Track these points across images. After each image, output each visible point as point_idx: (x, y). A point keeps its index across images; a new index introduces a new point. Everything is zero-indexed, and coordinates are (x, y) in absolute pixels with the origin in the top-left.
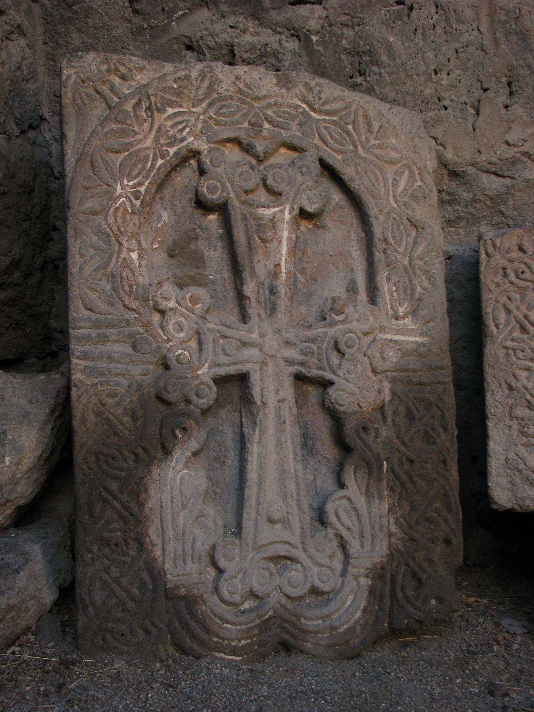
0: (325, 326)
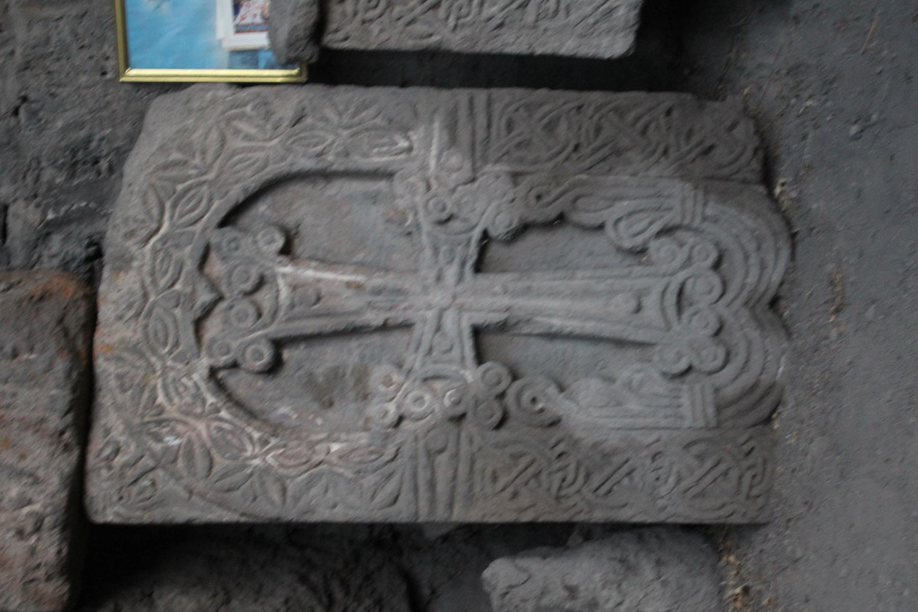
0: (420, 234)
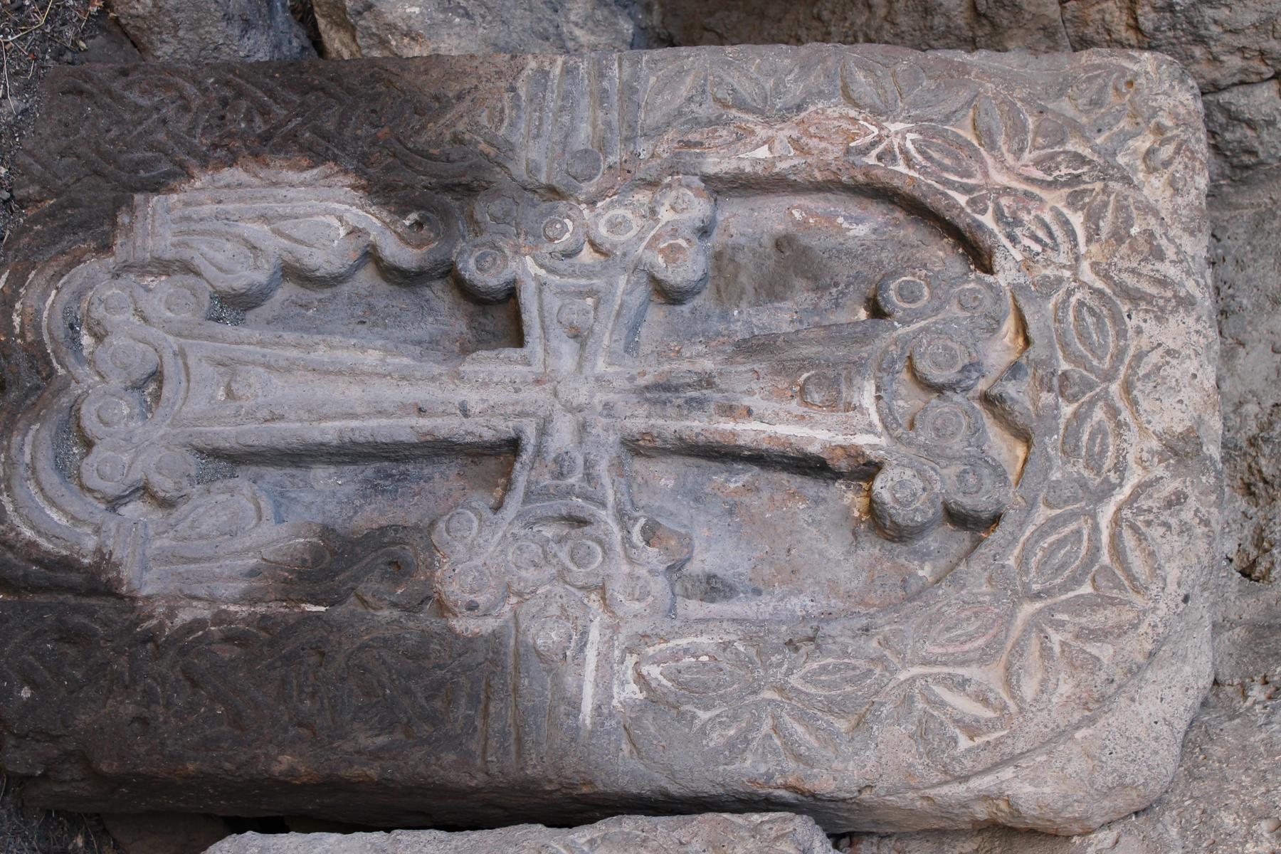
0: (618, 503)
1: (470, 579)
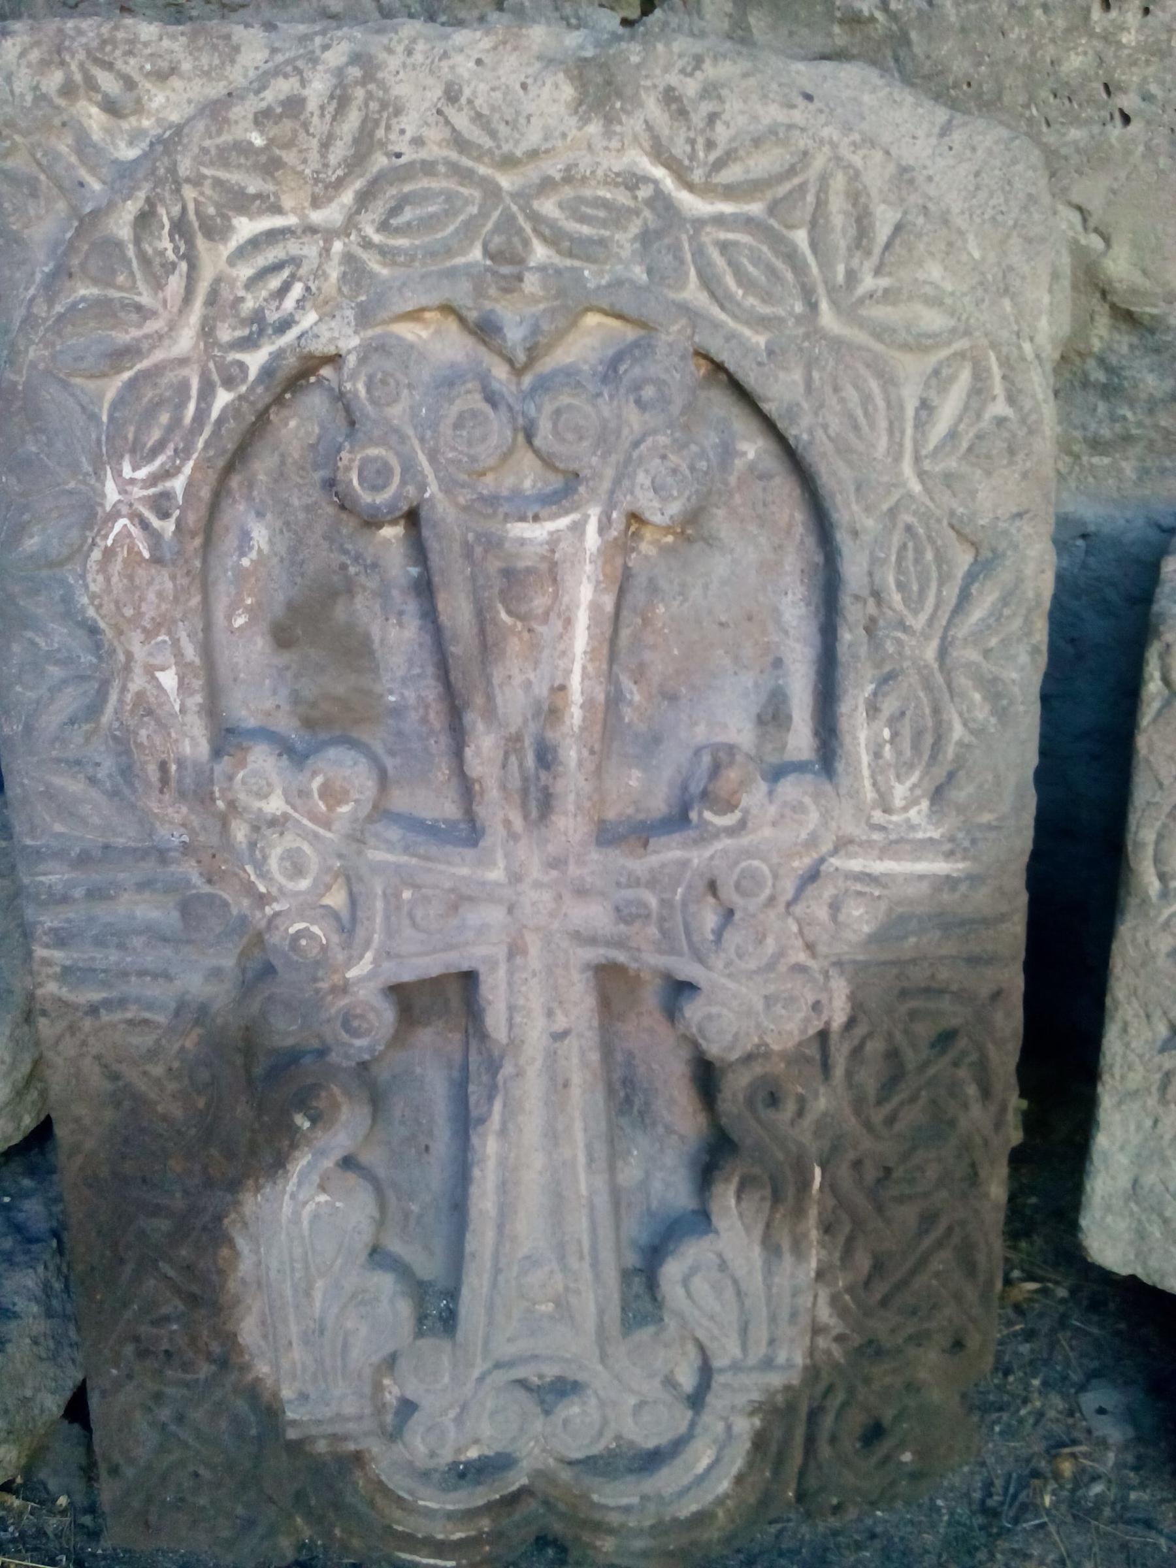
0: (684, 845)
1: (783, 1012)
